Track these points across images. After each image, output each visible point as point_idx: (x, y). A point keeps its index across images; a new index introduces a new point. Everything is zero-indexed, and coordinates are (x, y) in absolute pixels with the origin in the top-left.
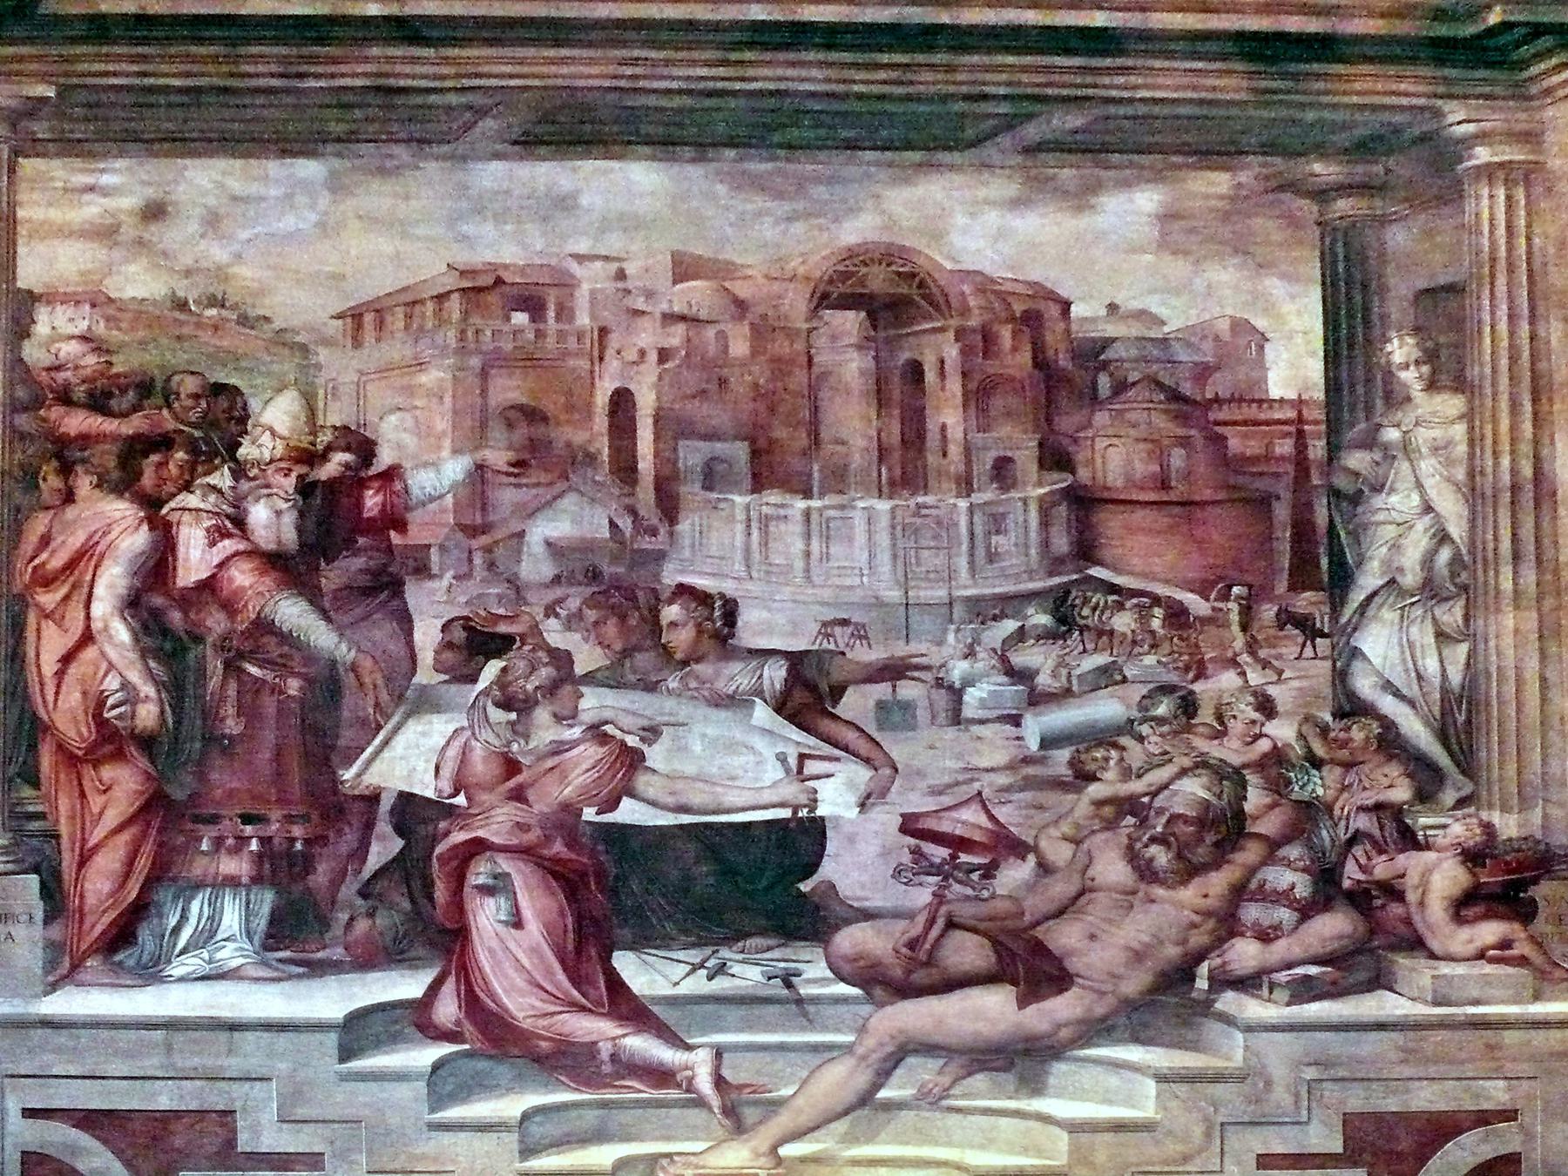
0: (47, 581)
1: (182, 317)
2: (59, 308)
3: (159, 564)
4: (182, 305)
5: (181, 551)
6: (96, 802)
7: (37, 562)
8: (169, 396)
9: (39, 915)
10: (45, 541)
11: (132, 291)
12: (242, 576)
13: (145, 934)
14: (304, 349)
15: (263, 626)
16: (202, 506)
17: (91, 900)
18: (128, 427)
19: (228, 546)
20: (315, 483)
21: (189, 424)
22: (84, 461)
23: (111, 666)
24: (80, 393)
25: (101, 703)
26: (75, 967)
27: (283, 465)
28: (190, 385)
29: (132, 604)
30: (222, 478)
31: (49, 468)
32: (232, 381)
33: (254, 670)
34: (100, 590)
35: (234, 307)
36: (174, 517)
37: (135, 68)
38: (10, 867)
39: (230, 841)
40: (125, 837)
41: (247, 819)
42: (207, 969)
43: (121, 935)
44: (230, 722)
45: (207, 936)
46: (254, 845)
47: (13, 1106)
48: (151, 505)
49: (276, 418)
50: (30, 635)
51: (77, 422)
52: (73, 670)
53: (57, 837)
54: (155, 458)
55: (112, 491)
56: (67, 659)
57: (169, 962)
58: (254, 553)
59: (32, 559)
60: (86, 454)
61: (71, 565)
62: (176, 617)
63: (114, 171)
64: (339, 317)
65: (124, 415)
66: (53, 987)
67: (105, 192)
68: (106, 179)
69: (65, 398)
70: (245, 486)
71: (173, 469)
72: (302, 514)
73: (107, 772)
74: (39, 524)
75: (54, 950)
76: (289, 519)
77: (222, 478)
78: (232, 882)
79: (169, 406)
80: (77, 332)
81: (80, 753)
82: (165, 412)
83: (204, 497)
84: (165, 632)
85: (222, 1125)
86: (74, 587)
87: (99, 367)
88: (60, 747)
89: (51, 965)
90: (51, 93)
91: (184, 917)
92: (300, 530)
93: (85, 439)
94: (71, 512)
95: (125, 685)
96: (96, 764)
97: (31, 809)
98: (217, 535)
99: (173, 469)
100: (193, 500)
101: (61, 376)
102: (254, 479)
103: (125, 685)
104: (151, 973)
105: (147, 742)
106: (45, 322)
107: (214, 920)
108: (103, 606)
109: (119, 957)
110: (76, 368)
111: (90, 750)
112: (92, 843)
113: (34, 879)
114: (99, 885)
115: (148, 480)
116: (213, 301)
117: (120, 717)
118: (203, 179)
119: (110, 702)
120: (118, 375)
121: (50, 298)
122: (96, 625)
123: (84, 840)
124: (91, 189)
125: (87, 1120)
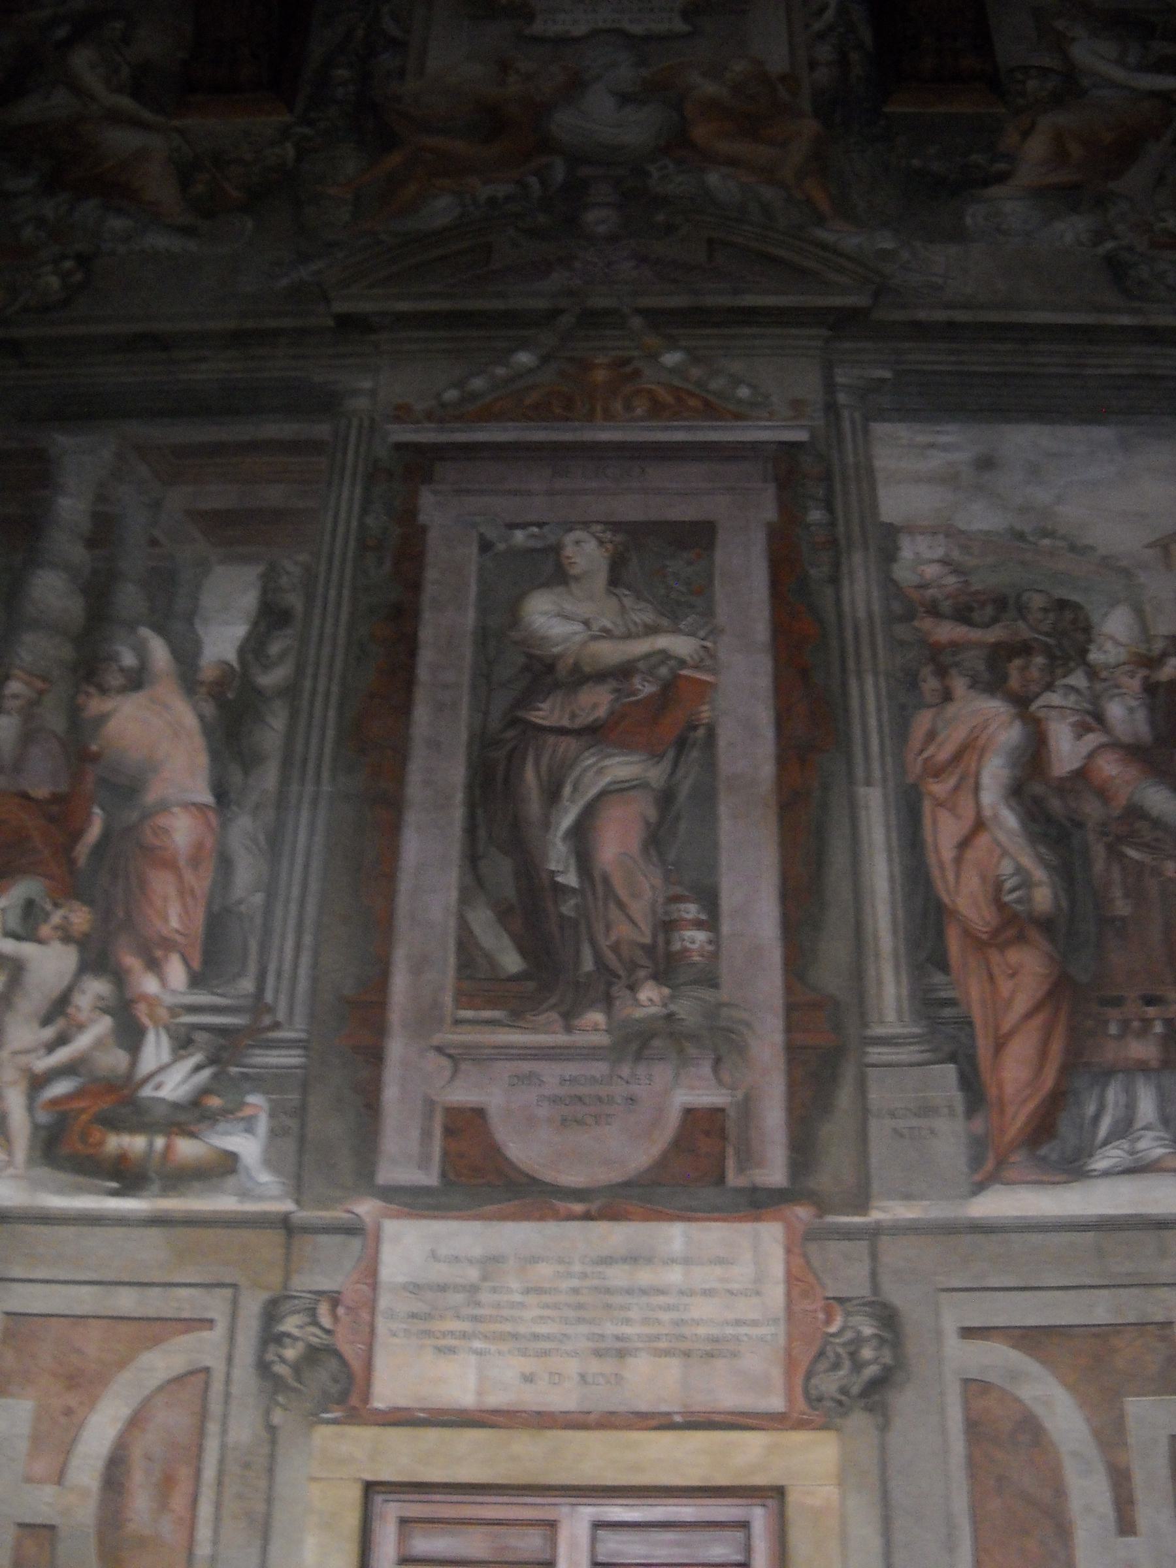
0: (938, 773)
1: (1023, 545)
2: (919, 538)
3: (1034, 755)
4: (1021, 536)
5: (1052, 743)
6: (1005, 987)
7: (925, 755)
8: (1022, 611)
9: (960, 1108)
10: (931, 736)
11: (977, 525)
12: (1109, 767)
13: (1065, 1127)
14: (1126, 573)
15: (1135, 812)
16: (1064, 703)
17: (1009, 1089)
18: (994, 635)
19: (1093, 740)
20: (1158, 684)
21: (1040, 633)
22: (957, 664)
23: (1005, 853)
24: (946, 606)
25: (998, 886)
26: (1001, 1163)
27: (1127, 668)
28: (1037, 601)
29: (1016, 792)
30: (1078, 679)
31: (927, 671)
32: (1075, 597)
33: (1133, 853)
34: (986, 779)
35: (1063, 538)
36: (1042, 714)
37: (953, 358)
38: (927, 1056)
39: (1136, 1024)
40: (1038, 1021)
41: (1150, 1001)
42: (1128, 1161)
43: (1042, 1129)
44: (1119, 903)
45: (1125, 1128)
46: (1158, 1028)
47: (950, 1324)
48: (1021, 702)
49: (1115, 631)
50: (927, 821)
51: (946, 631)
52: (970, 855)
53: (970, 1024)
54: (1018, 662)
55: (984, 691)
56: (964, 844)
57: (1091, 1156)
58: (1115, 745)
59: (922, 751)
60: (957, 659)
61: (957, 757)
62: (1055, 805)
63: (948, 433)
64: (1149, 546)
65: (987, 626)
66: (979, 1188)
67: (945, 448)
68: (943, 439)
69: (934, 610)
70: (1099, 686)
71: (1035, 673)
72: (1152, 709)
73: (1014, 956)
74: (923, 721)
75: (978, 1149)
76: (1141, 715)
77: (1078, 679)
78: (1143, 1068)
79: (1024, 619)
80: (936, 556)
81: (985, 937)
82: (1020, 623)
83: (1066, 695)
84: (1049, 820)
85: (1163, 1339)
86: (962, 778)
87: (960, 585)
88: (967, 933)
89: (976, 1161)
90: (888, 374)
91: (1101, 1108)
92: (1152, 723)
93: (955, 646)
94: (951, 709)
95: (1019, 870)
96: (1002, 947)
97: (943, 994)
98: (1082, 730)
99: (1035, 673)
100: (1055, 698)
101: (930, 592)
102: (1105, 680)
103: (1019, 870)
104: (1073, 1169)
105: (1046, 925)
106: (908, 549)
107: (1131, 1107)
108: (991, 794)
109: (1043, 1151)
110: (940, 587)
111: (995, 933)
112: (1006, 1027)
113: (950, 1070)
114: (1017, 1073)
115: (1014, 682)
116: (1046, 533)
117: (1019, 901)
118: (1021, 440)
119: (1008, 885)
120: (977, 592)
121: (910, 529)
122: (987, 813)
123: (997, 1028)
124: (932, 446)
125: (1030, 1339)
